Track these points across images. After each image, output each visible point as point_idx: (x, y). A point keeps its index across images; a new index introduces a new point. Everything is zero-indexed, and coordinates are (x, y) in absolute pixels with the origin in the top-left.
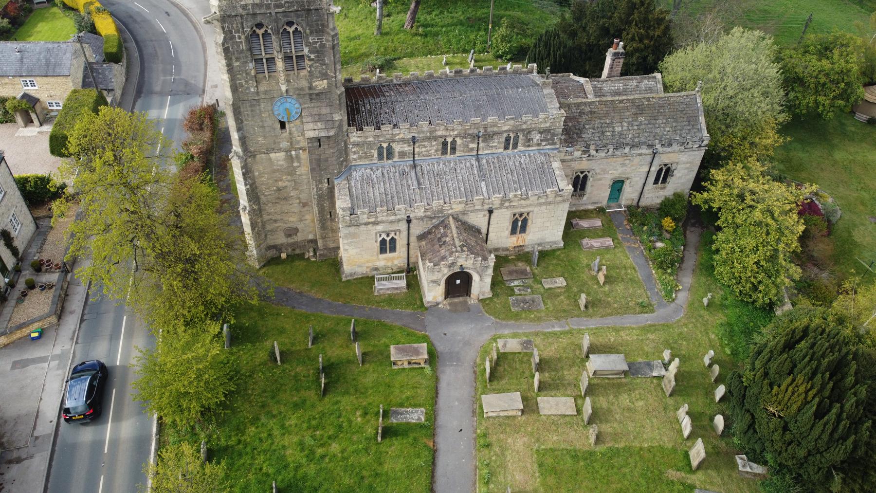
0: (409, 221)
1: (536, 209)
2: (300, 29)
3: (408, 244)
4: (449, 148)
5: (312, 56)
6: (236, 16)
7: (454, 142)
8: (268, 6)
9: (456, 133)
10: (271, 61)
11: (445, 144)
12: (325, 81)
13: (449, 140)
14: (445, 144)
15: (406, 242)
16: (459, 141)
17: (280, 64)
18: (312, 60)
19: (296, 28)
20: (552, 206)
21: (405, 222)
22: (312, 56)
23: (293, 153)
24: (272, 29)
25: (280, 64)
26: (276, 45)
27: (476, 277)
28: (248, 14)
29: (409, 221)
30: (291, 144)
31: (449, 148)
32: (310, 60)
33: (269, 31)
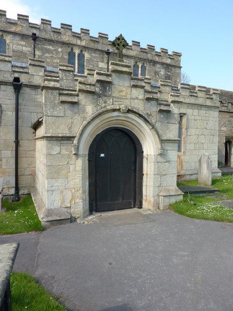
0: (17, 85)
1: (189, 111)
3: (17, 142)
4: (76, 61)
7: (81, 56)
9: (83, 43)
11: (71, 55)
13: (77, 51)
14: (71, 55)
15: (14, 138)
16: (87, 55)
20: (203, 112)
21: (10, 90)
27: (150, 147)
29: (17, 85)
31: (76, 61)
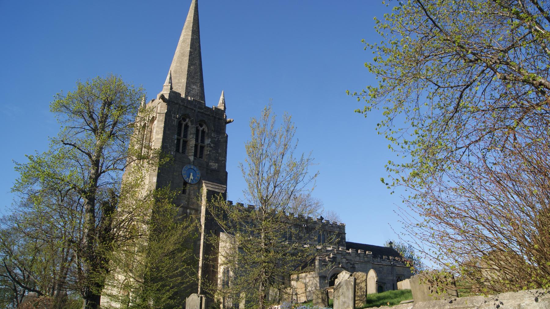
2: (206, 130)
5: (212, 145)
6: (177, 104)
8: (195, 106)
10: (185, 142)
12: (217, 164)
17: (192, 143)
18: (211, 147)
19: (204, 129)
22: (212, 145)
23: (188, 211)
24: (192, 121)
25: (192, 143)
26: (192, 130)
28: (183, 105)
30: (188, 204)
32: (211, 147)
33: (189, 124)
